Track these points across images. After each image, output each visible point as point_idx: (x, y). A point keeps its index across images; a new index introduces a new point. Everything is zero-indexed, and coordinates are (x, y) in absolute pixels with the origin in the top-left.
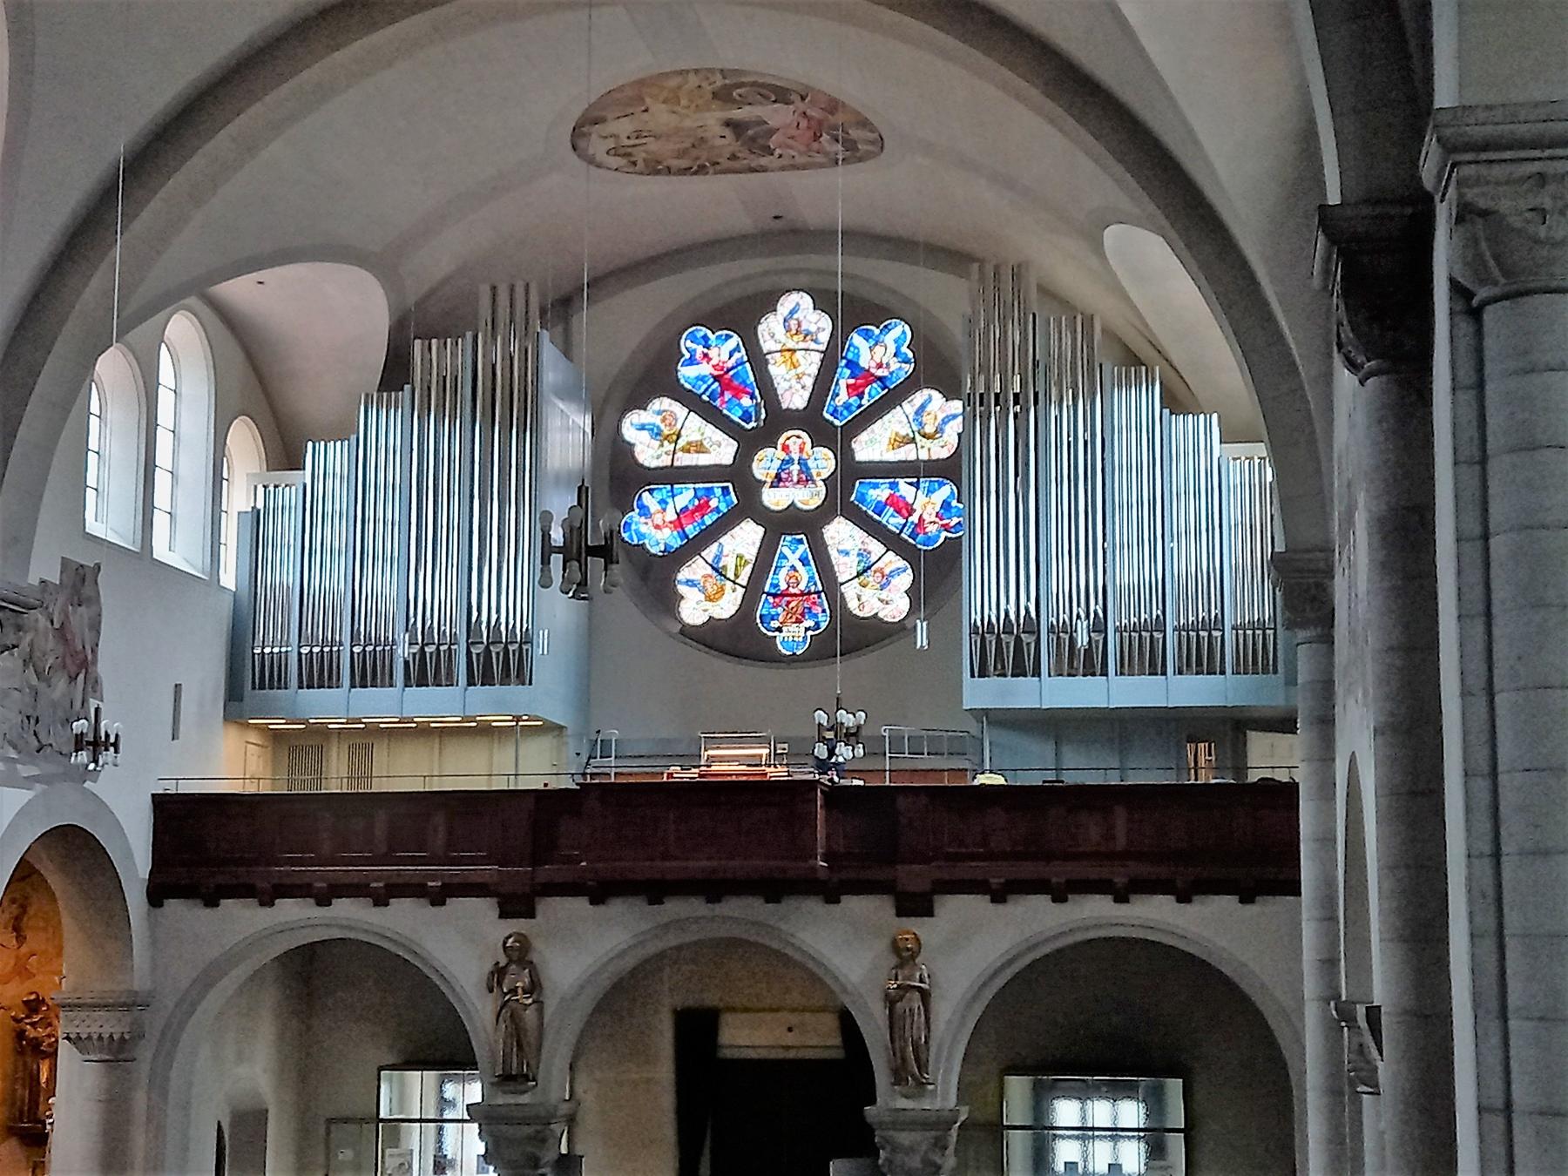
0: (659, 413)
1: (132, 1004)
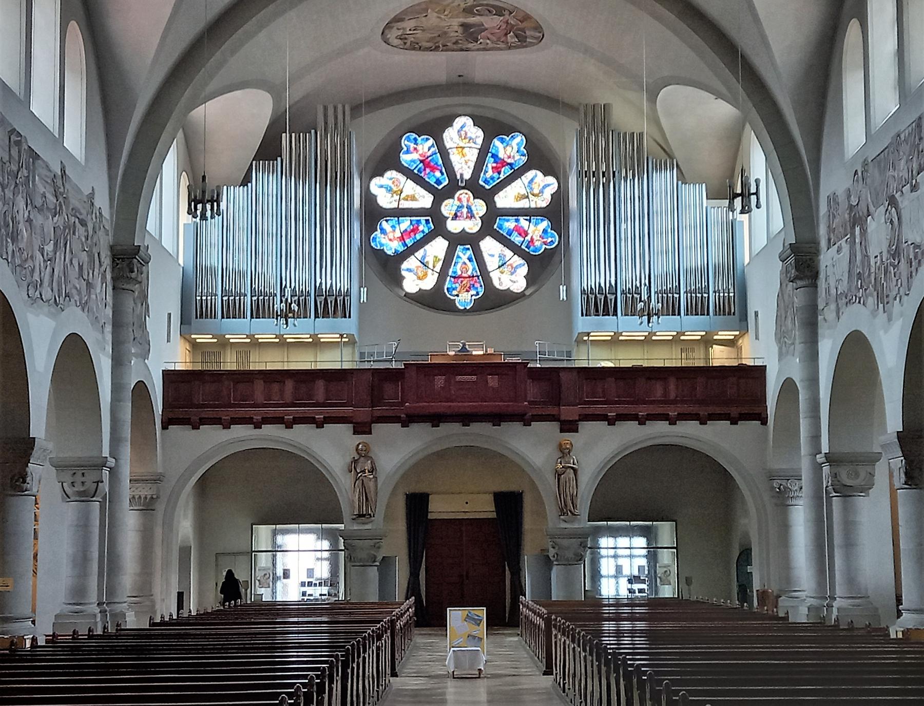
0: (391, 179)
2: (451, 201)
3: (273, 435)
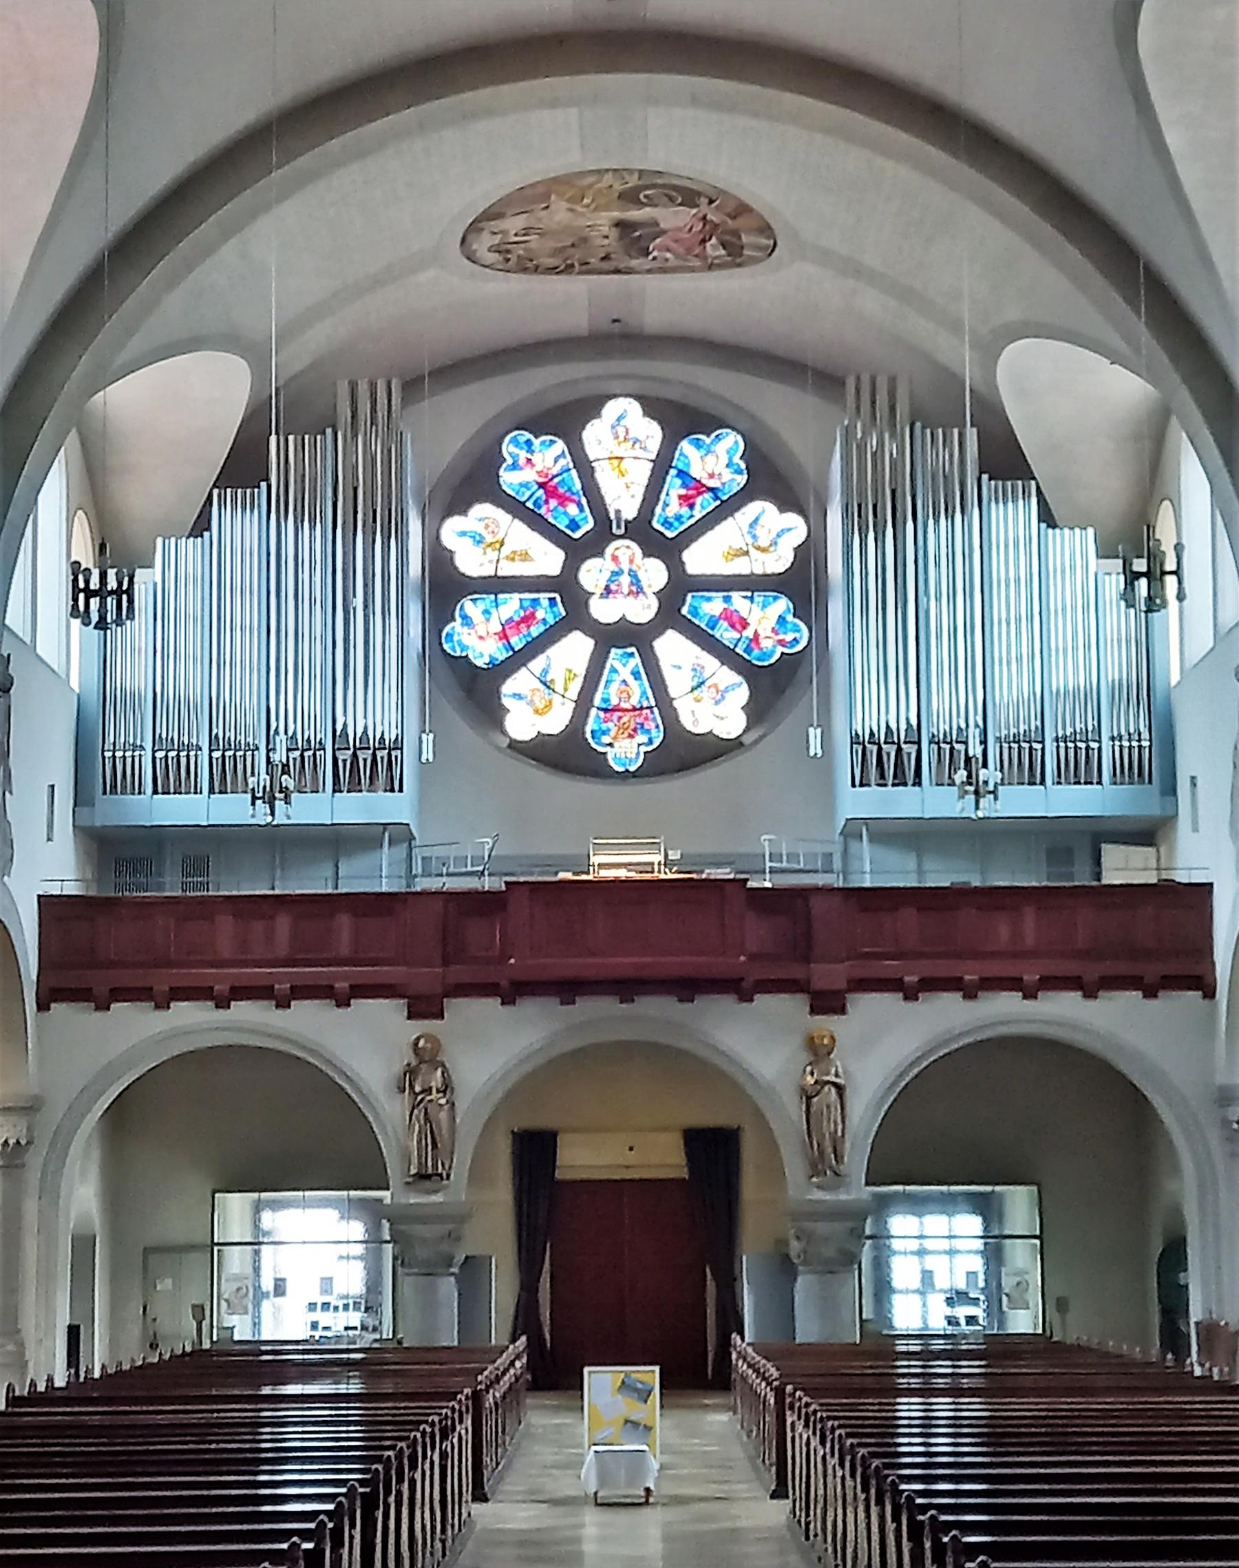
3: (250, 1019)
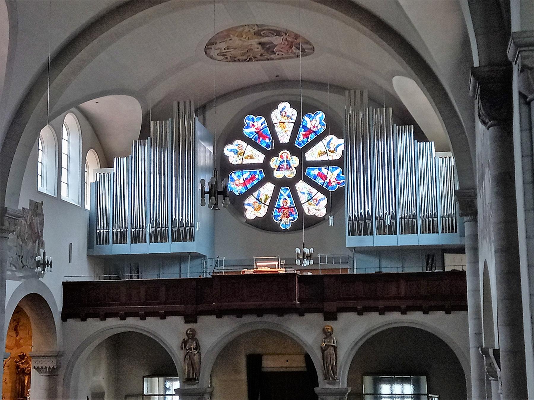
0: (237, 145)
1: (58, 355)
2: (275, 158)
